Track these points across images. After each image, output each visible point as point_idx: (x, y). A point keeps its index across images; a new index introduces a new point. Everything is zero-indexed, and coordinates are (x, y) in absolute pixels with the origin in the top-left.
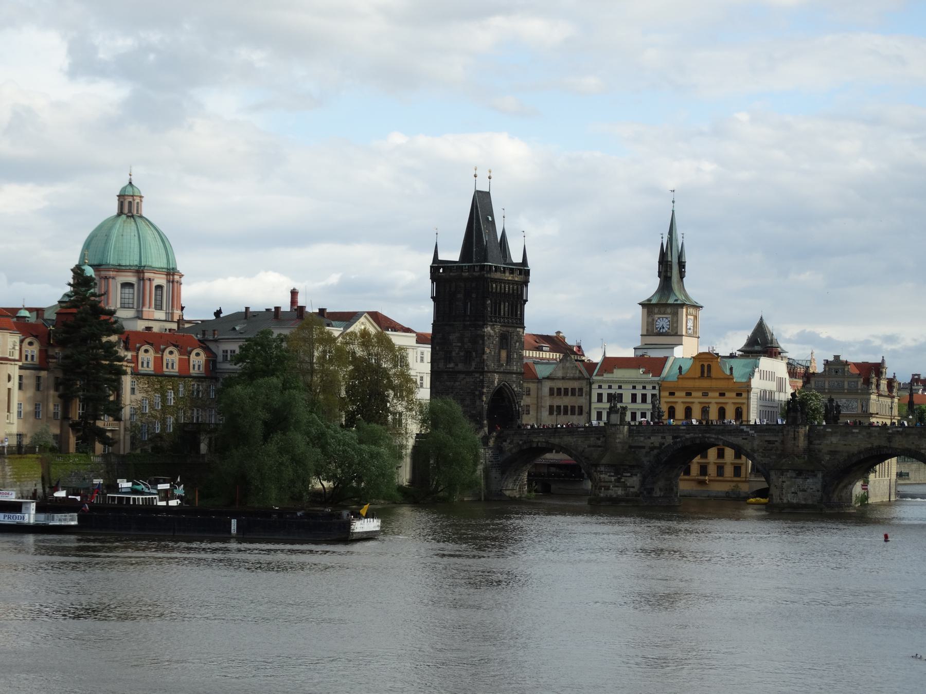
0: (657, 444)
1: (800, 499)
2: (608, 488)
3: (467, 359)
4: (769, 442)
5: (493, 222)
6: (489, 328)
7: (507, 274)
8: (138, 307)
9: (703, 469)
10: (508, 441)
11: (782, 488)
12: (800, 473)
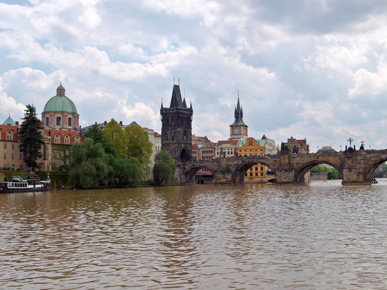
0: (237, 164)
1: (287, 180)
2: (220, 179)
3: (173, 139)
4: (275, 161)
5: (180, 95)
7: (185, 111)
8: (63, 125)
9: (251, 174)
10: (187, 165)
11: (281, 176)
12: (286, 171)
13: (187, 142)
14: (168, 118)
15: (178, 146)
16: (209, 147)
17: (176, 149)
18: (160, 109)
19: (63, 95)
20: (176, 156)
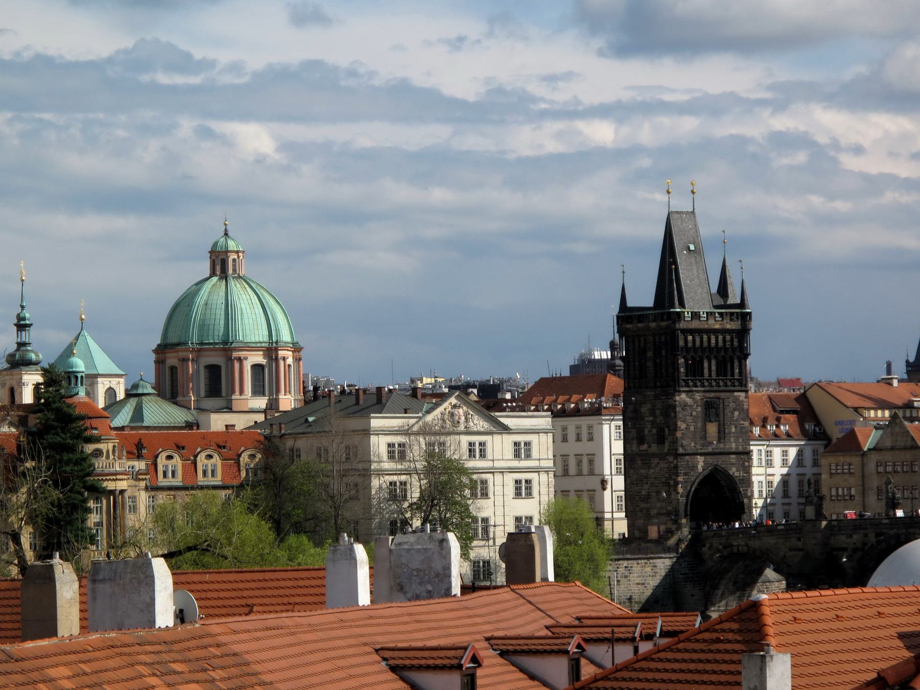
3: (661, 440)
6: (683, 396)
7: (711, 321)
10: (708, 545)
13: (721, 446)
16: (903, 444)
17: (670, 478)
18: (615, 309)
19: (234, 270)
20: (670, 508)
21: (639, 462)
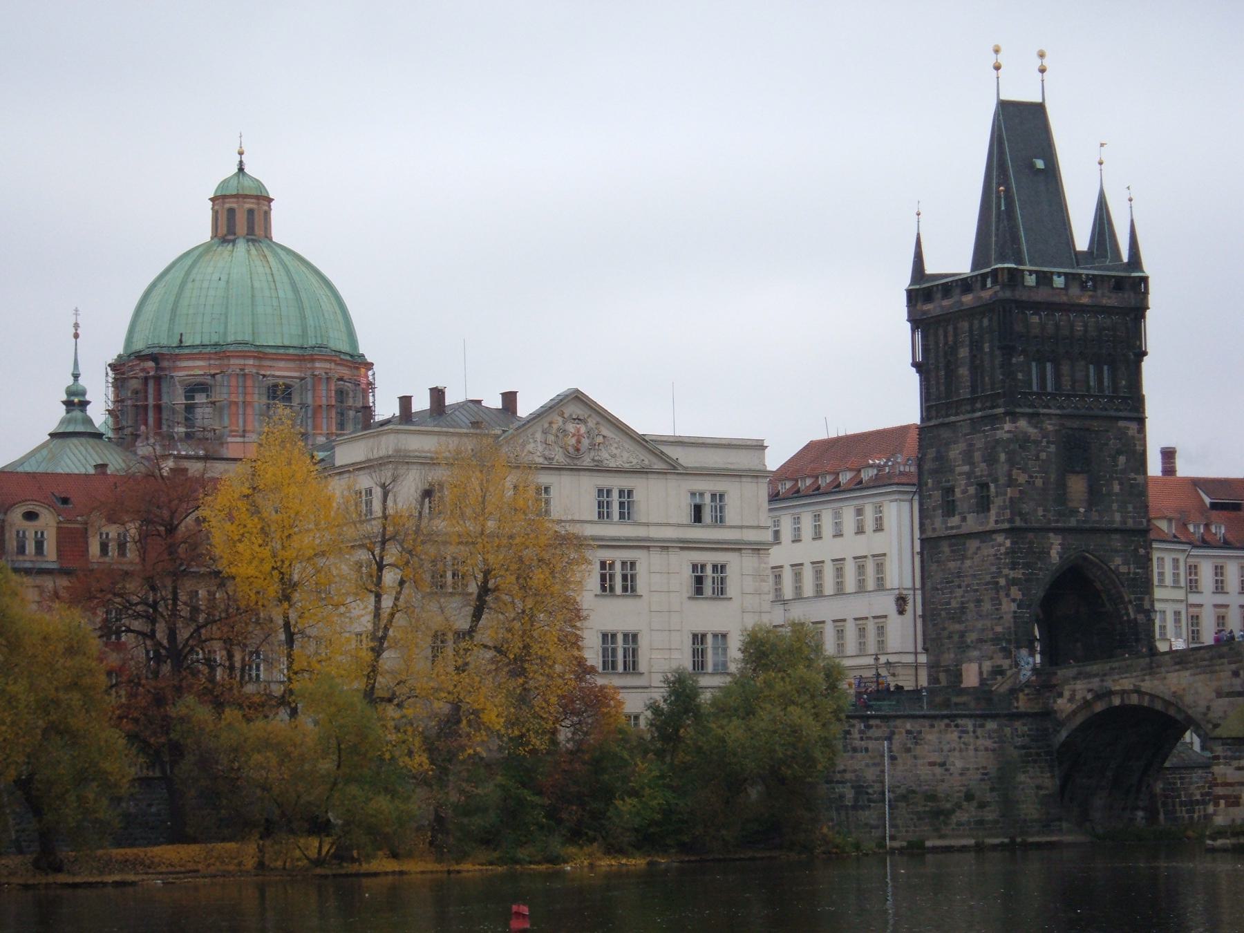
3: (983, 504)
5: (1051, 174)
7: (1075, 290)
10: (1067, 694)
13: (1095, 516)
14: (954, 349)
15: (1011, 552)
18: (904, 279)
20: (999, 629)
21: (946, 549)
